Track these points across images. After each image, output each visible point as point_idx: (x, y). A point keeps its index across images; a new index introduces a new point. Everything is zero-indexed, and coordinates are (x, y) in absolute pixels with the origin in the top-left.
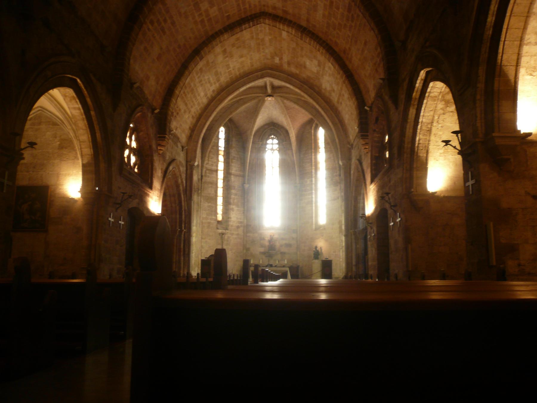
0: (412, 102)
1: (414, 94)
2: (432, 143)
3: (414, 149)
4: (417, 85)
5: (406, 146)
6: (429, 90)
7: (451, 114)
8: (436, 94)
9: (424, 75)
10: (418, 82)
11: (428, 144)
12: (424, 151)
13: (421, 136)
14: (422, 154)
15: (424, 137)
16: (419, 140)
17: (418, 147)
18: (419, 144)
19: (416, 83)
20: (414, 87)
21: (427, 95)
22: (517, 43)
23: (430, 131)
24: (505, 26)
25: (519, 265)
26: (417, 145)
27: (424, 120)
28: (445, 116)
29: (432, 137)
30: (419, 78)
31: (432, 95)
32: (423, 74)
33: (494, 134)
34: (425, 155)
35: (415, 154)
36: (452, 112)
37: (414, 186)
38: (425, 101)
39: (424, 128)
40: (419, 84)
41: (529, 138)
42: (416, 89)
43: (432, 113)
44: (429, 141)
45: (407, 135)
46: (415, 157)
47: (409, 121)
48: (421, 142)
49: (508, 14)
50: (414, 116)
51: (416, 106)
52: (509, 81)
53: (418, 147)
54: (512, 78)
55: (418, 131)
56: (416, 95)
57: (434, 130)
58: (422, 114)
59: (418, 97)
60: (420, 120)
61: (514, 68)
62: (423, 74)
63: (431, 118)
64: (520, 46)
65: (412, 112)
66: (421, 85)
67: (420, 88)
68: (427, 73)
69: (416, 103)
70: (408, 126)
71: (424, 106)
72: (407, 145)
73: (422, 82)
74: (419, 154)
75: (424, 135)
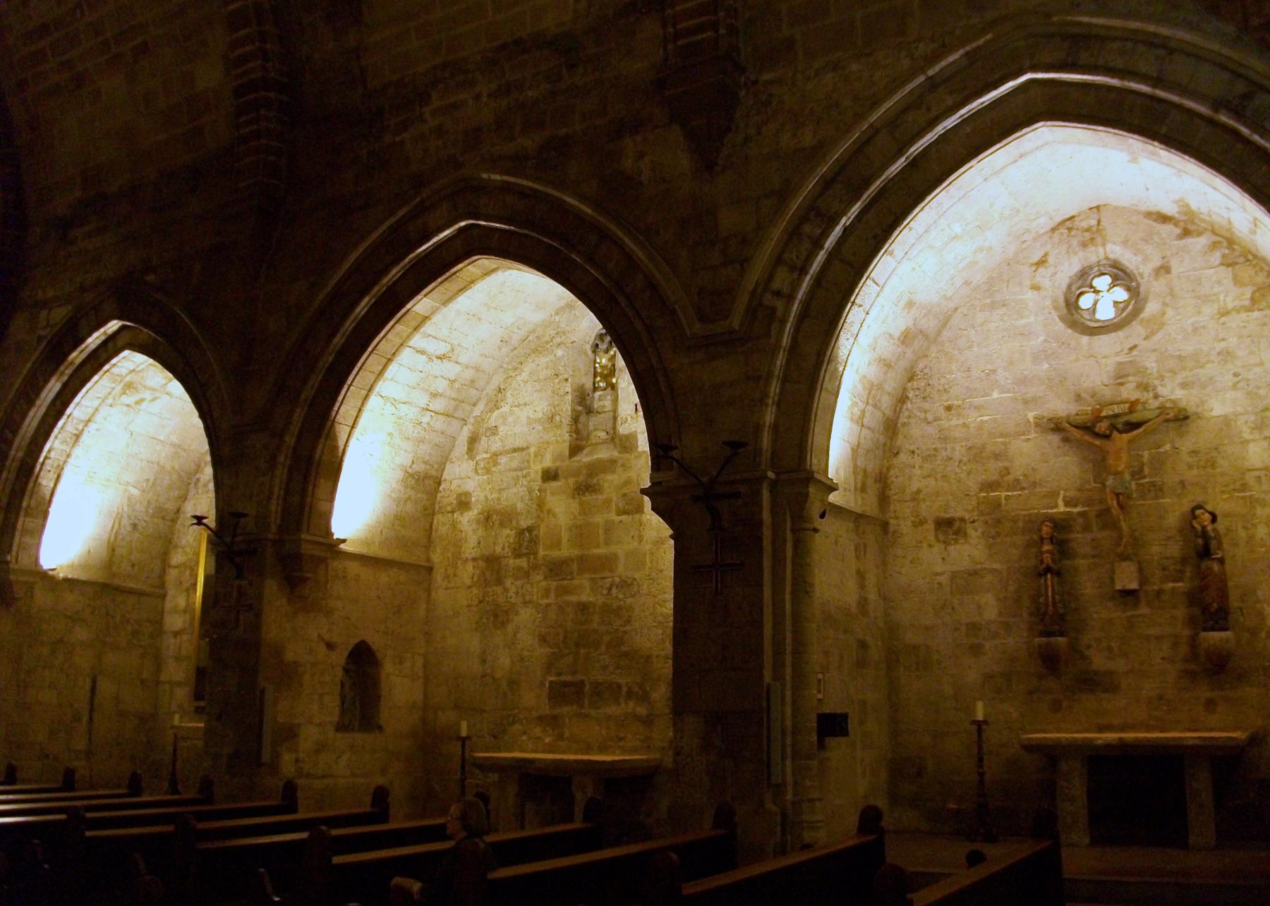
0: (62, 368)
1: (74, 354)
2: (71, 461)
3: (33, 467)
4: (90, 340)
5: (12, 453)
6: (114, 361)
7: (125, 409)
8: (124, 371)
9: (115, 328)
10: (96, 335)
11: (65, 462)
12: (53, 476)
13: (57, 444)
14: (46, 481)
15: (64, 447)
16: (49, 451)
17: (43, 464)
18: (46, 458)
19: (90, 335)
20: (83, 340)
21: (106, 367)
22: (364, 392)
23: (77, 437)
24: (359, 365)
25: (297, 761)
26: (41, 459)
27: (76, 414)
28: (113, 410)
29: (78, 451)
30: (102, 330)
31: (115, 370)
32: (113, 326)
33: (304, 536)
34: (52, 485)
35: (33, 478)
36: (128, 406)
37: (15, 548)
38: (96, 378)
39: (69, 428)
40: (94, 340)
41: (342, 546)
42: (83, 346)
43: (96, 403)
44: (68, 456)
45: (22, 432)
46: (31, 485)
47: (38, 402)
48: (52, 455)
49: (370, 349)
50: (52, 395)
51: (65, 378)
52: (336, 447)
53: (43, 464)
54: (341, 444)
55: (56, 431)
56: (77, 356)
57: (84, 438)
58: (77, 399)
59: (78, 361)
60: (68, 411)
61: (348, 429)
62: (113, 326)
63: (91, 411)
64: (366, 397)
65: (53, 387)
66: (98, 342)
67: (93, 347)
68: (122, 328)
69: (69, 372)
70: (31, 413)
71: (88, 385)
72: (17, 452)
73: (103, 338)
74: (40, 480)
75: (64, 442)
